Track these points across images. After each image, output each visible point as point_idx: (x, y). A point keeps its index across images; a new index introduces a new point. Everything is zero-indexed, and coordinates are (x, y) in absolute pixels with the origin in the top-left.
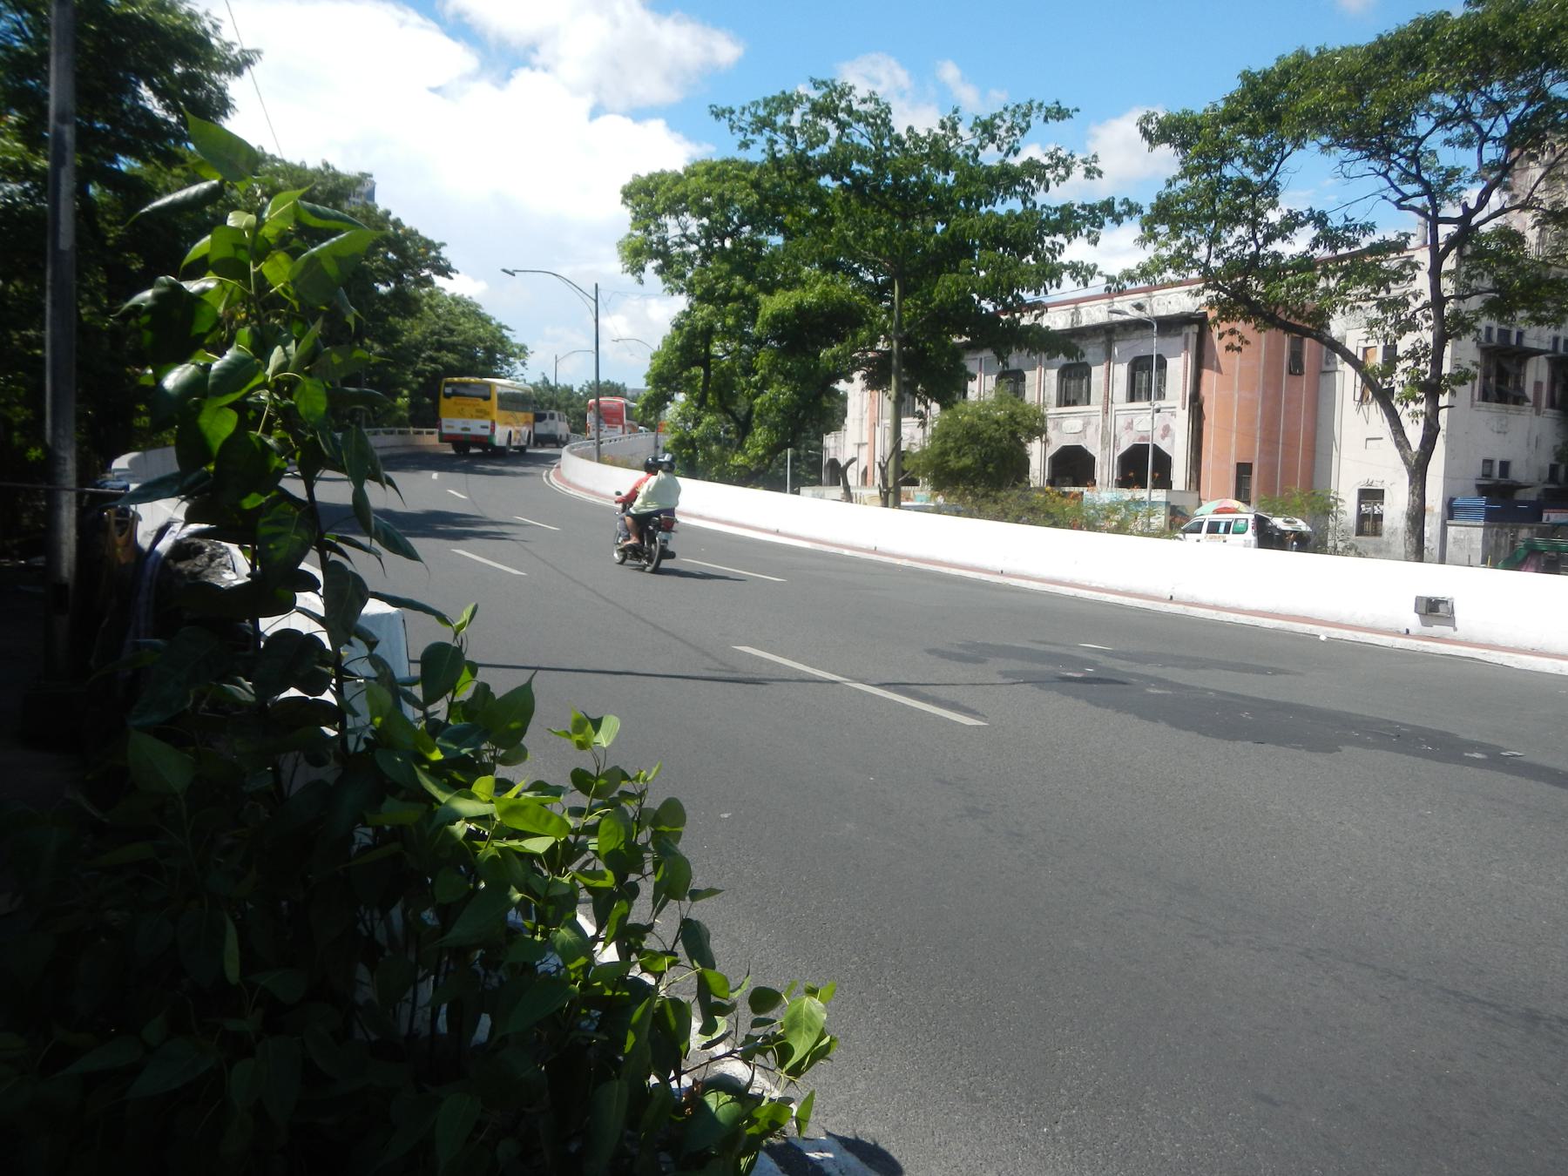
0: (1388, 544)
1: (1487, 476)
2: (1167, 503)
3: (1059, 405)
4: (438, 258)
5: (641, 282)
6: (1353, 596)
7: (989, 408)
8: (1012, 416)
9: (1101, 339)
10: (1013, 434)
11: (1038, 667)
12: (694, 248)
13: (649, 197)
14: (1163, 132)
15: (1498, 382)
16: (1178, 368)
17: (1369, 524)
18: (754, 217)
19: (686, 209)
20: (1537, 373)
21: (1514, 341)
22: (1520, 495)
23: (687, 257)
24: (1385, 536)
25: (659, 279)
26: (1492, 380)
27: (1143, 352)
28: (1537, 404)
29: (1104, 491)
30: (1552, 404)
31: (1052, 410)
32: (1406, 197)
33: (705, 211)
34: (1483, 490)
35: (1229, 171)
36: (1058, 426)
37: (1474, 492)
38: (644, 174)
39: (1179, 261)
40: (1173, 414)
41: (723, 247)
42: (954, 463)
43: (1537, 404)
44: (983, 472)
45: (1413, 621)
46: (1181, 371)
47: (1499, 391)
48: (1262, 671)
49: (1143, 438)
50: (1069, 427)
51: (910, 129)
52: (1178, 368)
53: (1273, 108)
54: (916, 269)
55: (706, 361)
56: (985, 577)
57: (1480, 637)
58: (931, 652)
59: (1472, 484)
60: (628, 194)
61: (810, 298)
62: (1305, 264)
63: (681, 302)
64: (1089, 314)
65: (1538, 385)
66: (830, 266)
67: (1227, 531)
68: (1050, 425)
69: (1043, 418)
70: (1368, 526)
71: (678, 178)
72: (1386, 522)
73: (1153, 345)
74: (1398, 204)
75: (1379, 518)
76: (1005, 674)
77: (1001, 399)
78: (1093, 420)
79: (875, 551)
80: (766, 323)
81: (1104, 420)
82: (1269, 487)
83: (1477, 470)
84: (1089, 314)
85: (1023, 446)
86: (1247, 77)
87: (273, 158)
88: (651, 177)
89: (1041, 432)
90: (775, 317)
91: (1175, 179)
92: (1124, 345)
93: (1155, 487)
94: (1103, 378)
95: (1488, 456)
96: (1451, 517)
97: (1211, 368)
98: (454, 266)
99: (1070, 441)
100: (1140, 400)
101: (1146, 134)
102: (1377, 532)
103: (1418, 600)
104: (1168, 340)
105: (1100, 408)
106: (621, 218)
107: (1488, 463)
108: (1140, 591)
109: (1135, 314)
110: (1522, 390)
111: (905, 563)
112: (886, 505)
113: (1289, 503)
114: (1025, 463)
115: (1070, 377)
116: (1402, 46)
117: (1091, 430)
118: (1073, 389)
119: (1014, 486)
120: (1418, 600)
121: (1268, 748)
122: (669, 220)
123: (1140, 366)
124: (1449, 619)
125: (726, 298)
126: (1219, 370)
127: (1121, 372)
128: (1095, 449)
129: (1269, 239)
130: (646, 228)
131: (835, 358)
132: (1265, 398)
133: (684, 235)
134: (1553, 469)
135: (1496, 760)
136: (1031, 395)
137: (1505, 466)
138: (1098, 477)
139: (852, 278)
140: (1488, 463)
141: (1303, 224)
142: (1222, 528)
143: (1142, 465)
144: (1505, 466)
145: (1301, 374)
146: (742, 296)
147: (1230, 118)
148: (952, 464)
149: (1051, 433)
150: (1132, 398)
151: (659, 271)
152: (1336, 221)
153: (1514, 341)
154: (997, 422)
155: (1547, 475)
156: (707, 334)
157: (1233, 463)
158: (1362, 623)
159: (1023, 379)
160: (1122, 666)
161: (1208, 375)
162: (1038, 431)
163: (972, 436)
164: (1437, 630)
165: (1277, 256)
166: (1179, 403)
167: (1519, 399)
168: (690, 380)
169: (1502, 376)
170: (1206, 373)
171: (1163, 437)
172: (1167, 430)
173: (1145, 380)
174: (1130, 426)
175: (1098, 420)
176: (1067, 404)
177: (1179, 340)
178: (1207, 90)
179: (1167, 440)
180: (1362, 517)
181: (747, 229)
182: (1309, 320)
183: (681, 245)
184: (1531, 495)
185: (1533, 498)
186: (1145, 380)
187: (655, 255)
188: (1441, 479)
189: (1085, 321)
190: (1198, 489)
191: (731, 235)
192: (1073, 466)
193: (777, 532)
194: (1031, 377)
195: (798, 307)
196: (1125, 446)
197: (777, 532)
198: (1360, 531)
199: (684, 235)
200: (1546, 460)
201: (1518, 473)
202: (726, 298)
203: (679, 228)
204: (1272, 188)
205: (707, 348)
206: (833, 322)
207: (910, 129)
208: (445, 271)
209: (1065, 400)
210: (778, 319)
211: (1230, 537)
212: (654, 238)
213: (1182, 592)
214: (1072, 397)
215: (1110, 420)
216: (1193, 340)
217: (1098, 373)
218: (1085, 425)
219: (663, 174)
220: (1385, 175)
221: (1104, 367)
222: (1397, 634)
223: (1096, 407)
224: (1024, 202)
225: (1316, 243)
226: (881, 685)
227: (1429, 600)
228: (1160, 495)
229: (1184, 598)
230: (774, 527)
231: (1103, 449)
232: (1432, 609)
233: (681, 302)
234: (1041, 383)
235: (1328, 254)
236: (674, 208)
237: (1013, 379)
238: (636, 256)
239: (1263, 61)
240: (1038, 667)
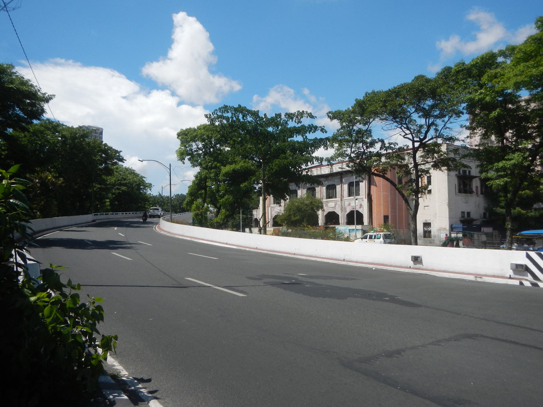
0: (433, 240)
1: (463, 217)
2: (362, 230)
3: (327, 198)
4: (119, 156)
5: (184, 163)
6: (394, 256)
7: (304, 200)
8: (311, 203)
9: (339, 177)
10: (312, 208)
11: (278, 280)
12: (201, 152)
13: (186, 136)
14: (334, 116)
15: (464, 187)
16: (363, 185)
17: (427, 234)
18: (218, 141)
19: (198, 140)
20: (476, 184)
21: (468, 174)
22: (475, 223)
23: (199, 155)
24: (432, 238)
25: (189, 162)
26: (462, 186)
27: (352, 181)
28: (477, 193)
29: (342, 228)
30: (482, 193)
31: (324, 200)
32: (406, 134)
33: (203, 140)
34: (462, 222)
35: (355, 128)
36: (327, 205)
37: (459, 222)
38: (184, 129)
39: (342, 155)
40: (363, 200)
41: (210, 151)
42: (293, 219)
43: (477, 193)
44: (301, 221)
45: (411, 263)
47: (464, 189)
48: (348, 279)
50: (330, 206)
51: (265, 115)
52: (363, 185)
53: (366, 108)
54: (269, 157)
55: (205, 188)
56: (289, 255)
57: (430, 268)
58: (246, 277)
59: (458, 220)
60: (179, 135)
61: (238, 167)
62: (379, 155)
63: (198, 169)
64: (335, 168)
65: (477, 187)
66: (245, 157)
67: (375, 238)
68: (324, 205)
69: (322, 203)
70: (427, 234)
71: (195, 130)
72: (432, 233)
73: (354, 179)
74: (404, 136)
75: (430, 232)
76: (264, 283)
77: (308, 197)
78: (338, 203)
79: (257, 248)
80: (224, 175)
81: (341, 203)
82: (394, 221)
83: (459, 215)
84: (335, 168)
85: (316, 212)
86: (356, 100)
87: (63, 125)
88: (187, 130)
89: (322, 207)
90: (226, 173)
91: (340, 129)
92: (346, 178)
93: (357, 224)
94: (340, 189)
95: (463, 211)
96: (452, 231)
98: (124, 158)
99: (331, 210)
100: (352, 196)
101: (329, 117)
102: (430, 237)
103: (412, 257)
105: (340, 199)
106: (177, 144)
107: (463, 213)
108: (335, 258)
109: (340, 170)
110: (472, 189)
111: (265, 252)
112: (261, 233)
113: (402, 228)
114: (317, 217)
115: (330, 189)
116: (395, 92)
117: (337, 206)
118: (331, 193)
119: (299, 226)
120: (412, 257)
121: (327, 299)
122: (194, 144)
123: (351, 185)
124: (421, 262)
125: (211, 168)
126: (376, 186)
127: (346, 187)
128: (338, 212)
129: (367, 147)
130: (185, 146)
131: (246, 186)
132: (391, 194)
133: (198, 148)
134: (485, 214)
135: (393, 300)
136: (318, 196)
137: (469, 214)
138: (340, 222)
139: (248, 163)
140: (463, 213)
141: (377, 142)
142: (373, 237)
143: (354, 218)
144: (469, 214)
146: (216, 167)
147: (353, 112)
148: (292, 219)
149: (325, 208)
150: (350, 194)
151: (189, 159)
152: (386, 142)
153: (468, 174)
154: (306, 205)
155: (482, 216)
156: (205, 179)
157: (382, 215)
158: (398, 265)
159: (315, 190)
160: (304, 279)
161: (372, 187)
162: (320, 206)
163: (299, 209)
164: (418, 266)
165: (370, 152)
166: (364, 197)
167: (471, 192)
168: (201, 194)
169: (465, 185)
170: (372, 187)
172: (361, 205)
173: (353, 190)
174: (349, 204)
176: (329, 198)
178: (347, 104)
180: (425, 232)
181: (218, 145)
182: (380, 172)
183: (197, 151)
184: (478, 223)
185: (479, 224)
186: (353, 190)
187: (188, 155)
188: (448, 219)
189: (335, 171)
190: (372, 224)
191: (212, 147)
192: (332, 218)
193: (227, 244)
194: (318, 189)
195: (234, 170)
196: (348, 211)
197: (227, 244)
198: (425, 236)
199: (198, 148)
200: (482, 211)
201: (473, 216)
202: (211, 168)
203: (196, 146)
204: (369, 132)
205: (206, 183)
206: (245, 175)
207: (265, 115)
208: (122, 160)
209: (329, 197)
210: (227, 174)
211: (376, 240)
212: (188, 149)
213: (347, 258)
214: (331, 196)
215: (343, 201)
217: (338, 187)
218: (336, 205)
219: (190, 129)
220: (401, 128)
221: (340, 185)
222: (407, 268)
223: (338, 198)
224: (306, 137)
225: (381, 148)
226: (224, 287)
227: (415, 257)
228: (359, 227)
229: (348, 260)
230: (226, 242)
231: (341, 212)
232: (416, 259)
233: (198, 169)
234: (321, 192)
235: (385, 152)
236: (194, 140)
237: (312, 191)
238: (182, 156)
239: (361, 97)
240: (278, 280)
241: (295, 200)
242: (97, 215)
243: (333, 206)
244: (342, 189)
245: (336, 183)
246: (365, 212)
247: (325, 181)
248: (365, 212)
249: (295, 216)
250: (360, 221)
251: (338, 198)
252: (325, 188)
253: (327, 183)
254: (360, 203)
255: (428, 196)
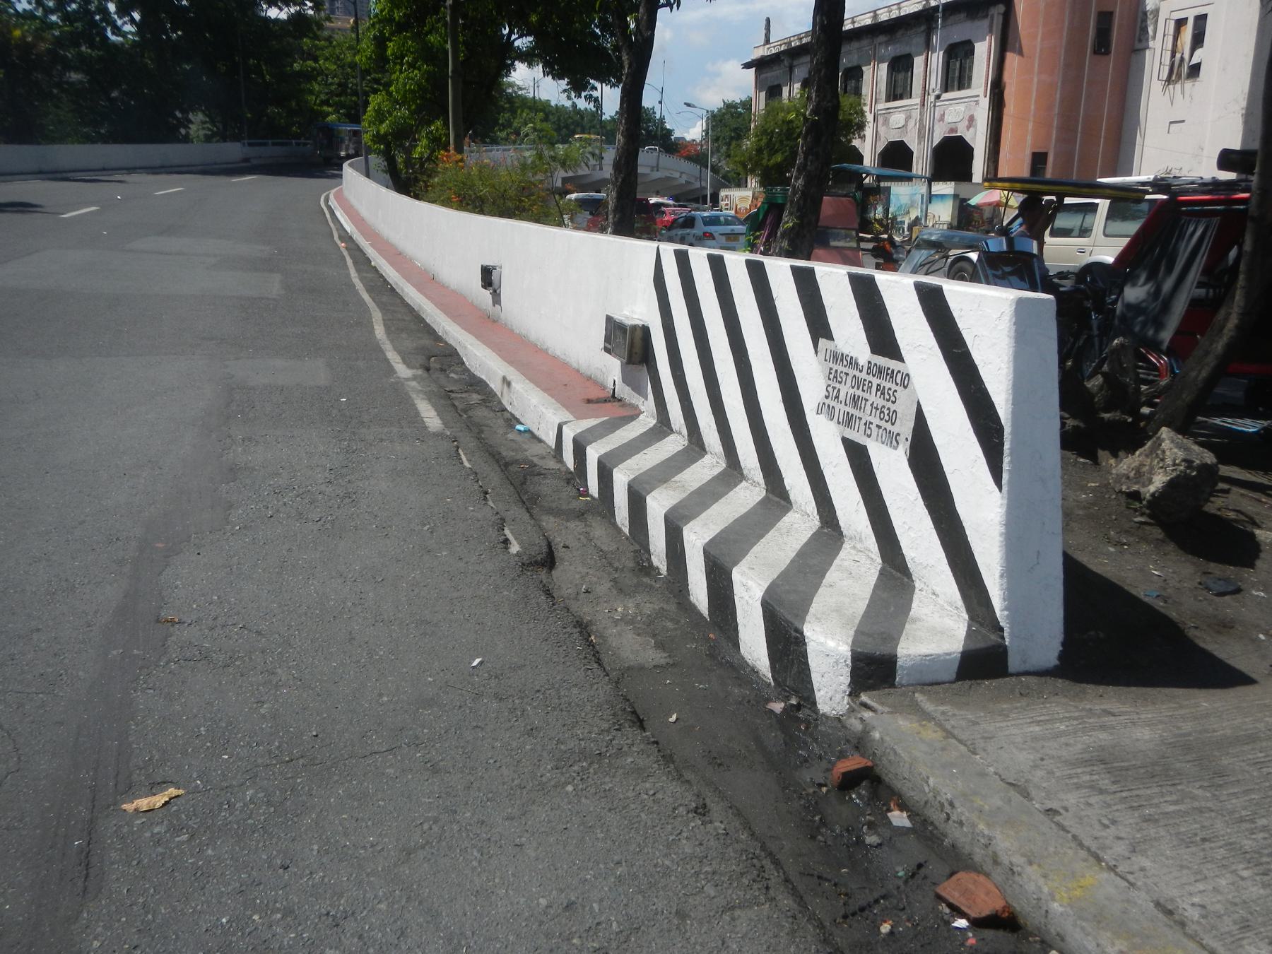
2: (955, 196)
3: (888, 100)
9: (923, 28)
16: (983, 51)
46: (985, 56)
49: (952, 130)
52: (983, 51)
73: (959, 31)
94: (922, 69)
97: (1013, 51)
100: (953, 90)
104: (978, 23)
115: (899, 71)
117: (911, 123)
126: (1021, 53)
127: (937, 59)
128: (913, 145)
145: (1107, 53)
161: (1011, 58)
166: (981, 91)
171: (968, 128)
172: (971, 119)
175: (916, 114)
177: (985, 23)
179: (972, 130)
196: (937, 140)
214: (899, 91)
216: (998, 21)
217: (918, 62)
218: (908, 118)
223: (915, 100)
231: (919, 143)
241: (776, 103)
242: (265, 144)
243: (902, 123)
244: (928, 66)
245: (913, 50)
246: (979, 142)
247: (887, 43)
248: (979, 142)
249: (770, 156)
250: (963, 174)
251: (915, 100)
252: (884, 67)
253: (891, 51)
254: (966, 113)
255: (1188, 84)
